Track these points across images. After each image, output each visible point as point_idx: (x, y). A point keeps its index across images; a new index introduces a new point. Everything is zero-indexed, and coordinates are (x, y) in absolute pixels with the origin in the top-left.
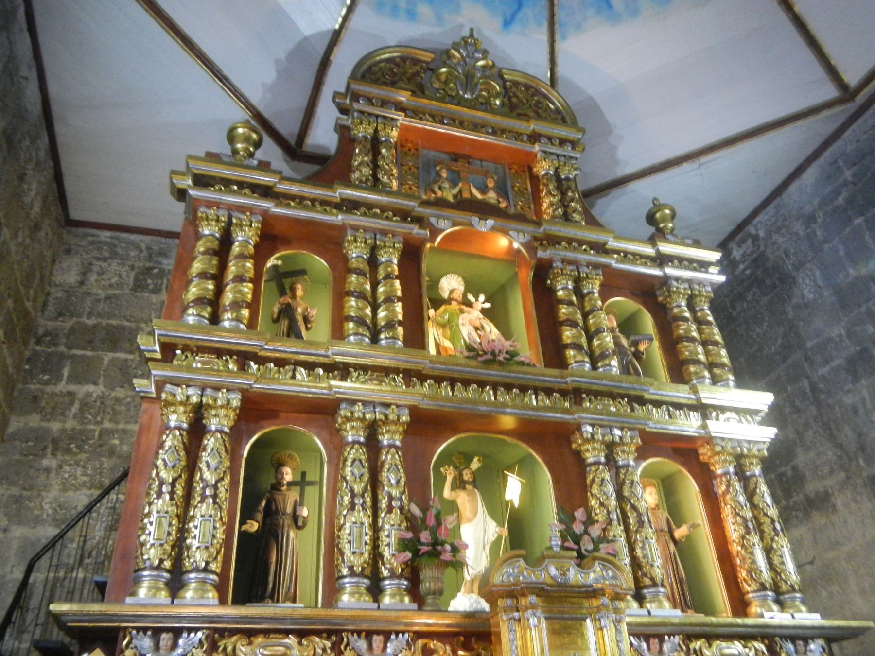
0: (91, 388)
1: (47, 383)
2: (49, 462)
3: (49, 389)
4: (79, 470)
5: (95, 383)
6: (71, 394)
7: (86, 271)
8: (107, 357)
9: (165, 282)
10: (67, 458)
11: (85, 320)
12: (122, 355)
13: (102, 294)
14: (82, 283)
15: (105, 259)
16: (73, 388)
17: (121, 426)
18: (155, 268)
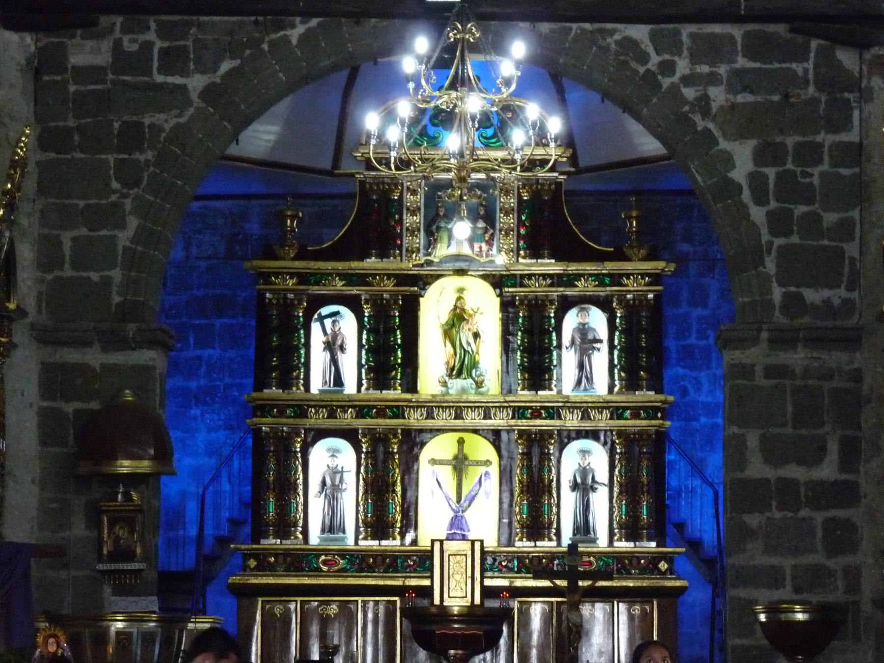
0: (211, 351)
1: (181, 350)
2: (195, 412)
3: (183, 354)
4: (216, 417)
5: (214, 348)
6: (199, 358)
7: (187, 248)
8: (218, 323)
9: (250, 247)
10: (206, 408)
11: (195, 292)
12: (227, 321)
13: (203, 264)
14: (187, 257)
15: (199, 232)
16: (199, 352)
17: (237, 381)
18: (239, 234)
